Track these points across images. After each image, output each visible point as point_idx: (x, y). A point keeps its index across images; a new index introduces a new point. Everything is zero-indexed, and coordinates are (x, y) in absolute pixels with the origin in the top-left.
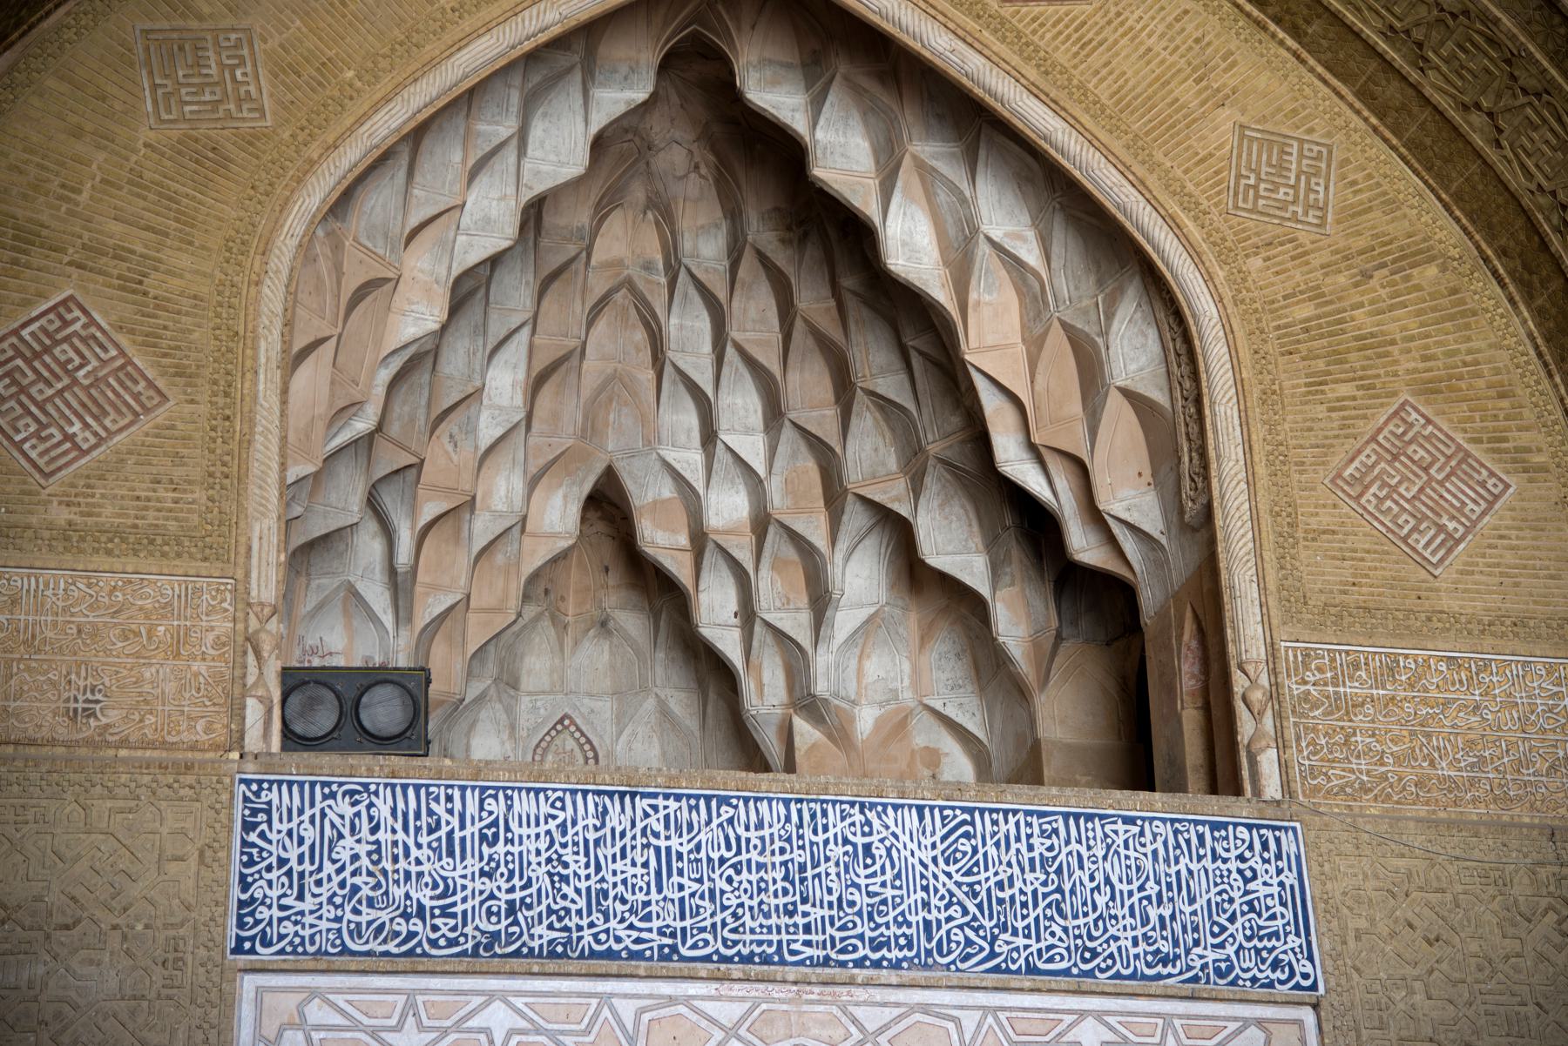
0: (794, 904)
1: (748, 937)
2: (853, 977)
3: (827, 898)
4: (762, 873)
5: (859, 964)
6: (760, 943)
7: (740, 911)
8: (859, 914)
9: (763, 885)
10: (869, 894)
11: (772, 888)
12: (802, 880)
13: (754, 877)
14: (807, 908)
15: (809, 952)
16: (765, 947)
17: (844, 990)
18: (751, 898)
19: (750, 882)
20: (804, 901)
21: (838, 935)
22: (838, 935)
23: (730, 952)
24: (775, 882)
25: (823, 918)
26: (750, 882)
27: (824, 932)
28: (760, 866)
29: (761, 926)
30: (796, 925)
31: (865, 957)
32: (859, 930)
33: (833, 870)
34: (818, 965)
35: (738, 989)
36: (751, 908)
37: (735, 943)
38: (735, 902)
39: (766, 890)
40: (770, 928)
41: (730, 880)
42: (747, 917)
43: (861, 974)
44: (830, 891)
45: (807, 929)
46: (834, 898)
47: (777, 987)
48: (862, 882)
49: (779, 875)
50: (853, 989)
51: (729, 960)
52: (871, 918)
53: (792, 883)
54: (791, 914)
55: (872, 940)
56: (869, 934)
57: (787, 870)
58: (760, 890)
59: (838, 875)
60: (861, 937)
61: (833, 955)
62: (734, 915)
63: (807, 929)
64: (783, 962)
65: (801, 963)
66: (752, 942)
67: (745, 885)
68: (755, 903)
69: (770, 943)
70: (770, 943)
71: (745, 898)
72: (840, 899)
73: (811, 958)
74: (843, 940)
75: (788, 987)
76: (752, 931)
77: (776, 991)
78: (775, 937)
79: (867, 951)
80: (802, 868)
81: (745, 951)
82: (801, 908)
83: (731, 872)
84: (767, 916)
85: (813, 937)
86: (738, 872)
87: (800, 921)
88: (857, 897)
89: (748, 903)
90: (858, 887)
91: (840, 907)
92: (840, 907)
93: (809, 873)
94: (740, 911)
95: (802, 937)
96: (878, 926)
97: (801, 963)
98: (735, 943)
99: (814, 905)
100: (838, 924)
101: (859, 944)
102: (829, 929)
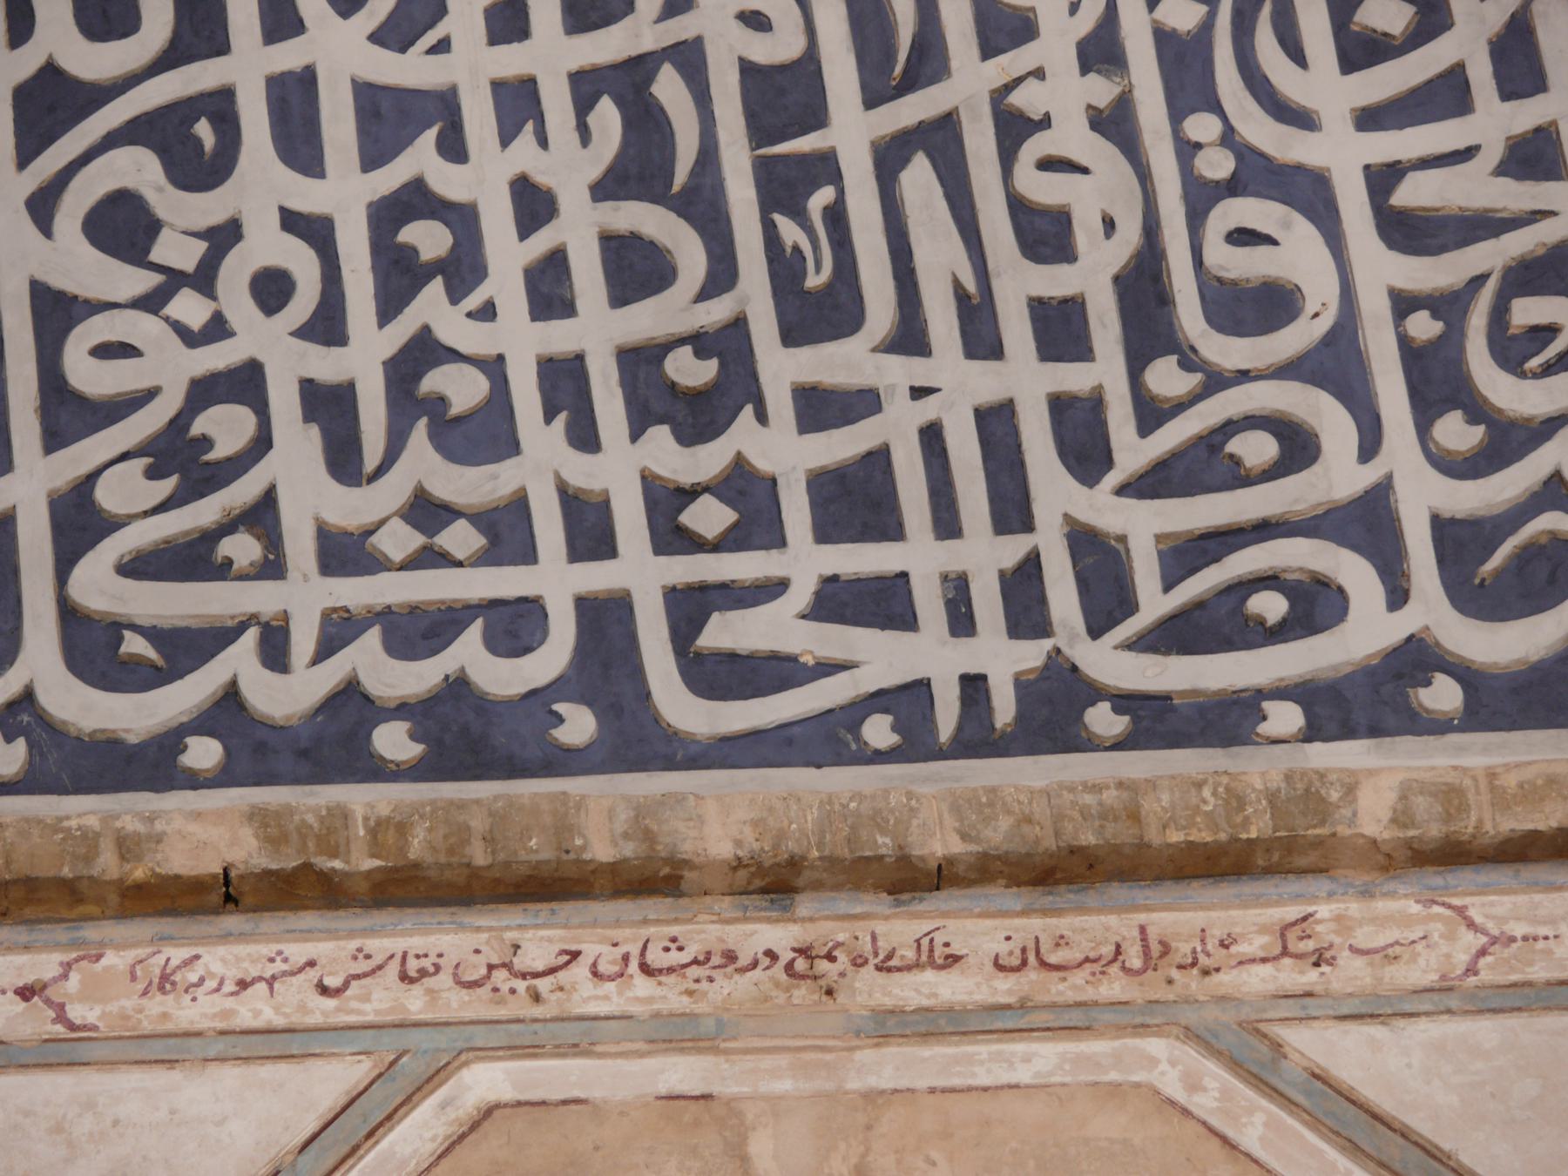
0: (729, 345)
1: (306, 596)
2: (1309, 796)
3: (1019, 282)
4: (421, 158)
5: (1369, 703)
6: (418, 631)
7: (227, 428)
8: (1336, 366)
9: (428, 238)
10: (1407, 231)
11: (508, 256)
12: (783, 187)
13: (346, 193)
14: (843, 362)
15: (881, 659)
16: (468, 653)
17: (1244, 917)
18: (327, 326)
19: (313, 230)
20: (818, 314)
21: (1143, 526)
22: (1143, 526)
23: (134, 715)
24: (534, 207)
25: (996, 423)
26: (313, 230)
27: (1013, 512)
28: (387, 118)
29: (426, 511)
30: (749, 491)
31: (1417, 658)
32: (1339, 475)
33: (1065, 96)
34: (978, 739)
35: (225, 970)
36: (329, 406)
37: (187, 648)
38: (170, 368)
39: (463, 269)
40: (506, 532)
41: (122, 227)
42: (297, 458)
43: (1377, 779)
44: (1046, 235)
45: (856, 501)
46: (1092, 276)
47: (605, 930)
48: (1342, 155)
49: (571, 162)
50: (1327, 908)
51: (152, 765)
52: (1436, 382)
53: (703, 207)
54: (699, 417)
55: (1458, 541)
56: (1422, 497)
57: (646, 122)
58: (399, 277)
59: (1115, 123)
60: (1368, 523)
61: (1110, 662)
62: (180, 460)
63: (856, 501)
64: (637, 742)
65: (829, 739)
66: (338, 631)
67: (267, 245)
68: (364, 357)
69: (515, 625)
70: (515, 625)
71: (262, 338)
72: (1143, 287)
73: (908, 701)
74: (1187, 553)
75: (705, 928)
76: (344, 553)
77: (589, 958)
78: (556, 580)
79: (1432, 611)
80: (782, 97)
81: (285, 697)
82: (781, 368)
83: (138, 169)
84: (485, 434)
85: (918, 557)
86: (199, 170)
87: (786, 453)
88: (1298, 254)
89: (288, 362)
90: (1310, 193)
91: (1149, 330)
92: (1149, 330)
93: (851, 130)
94: (227, 428)
95: (807, 560)
96: (1508, 440)
97: (829, 739)
98: (187, 648)
99: (909, 338)
100: (1133, 451)
101: (1354, 573)
102: (1054, 490)
